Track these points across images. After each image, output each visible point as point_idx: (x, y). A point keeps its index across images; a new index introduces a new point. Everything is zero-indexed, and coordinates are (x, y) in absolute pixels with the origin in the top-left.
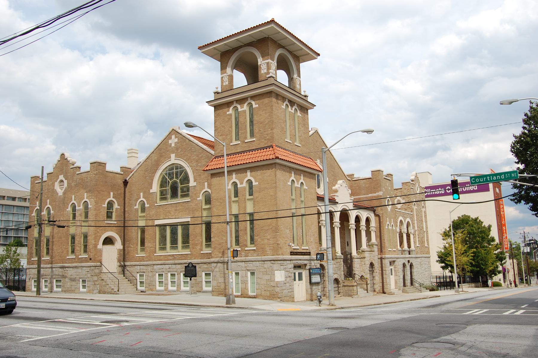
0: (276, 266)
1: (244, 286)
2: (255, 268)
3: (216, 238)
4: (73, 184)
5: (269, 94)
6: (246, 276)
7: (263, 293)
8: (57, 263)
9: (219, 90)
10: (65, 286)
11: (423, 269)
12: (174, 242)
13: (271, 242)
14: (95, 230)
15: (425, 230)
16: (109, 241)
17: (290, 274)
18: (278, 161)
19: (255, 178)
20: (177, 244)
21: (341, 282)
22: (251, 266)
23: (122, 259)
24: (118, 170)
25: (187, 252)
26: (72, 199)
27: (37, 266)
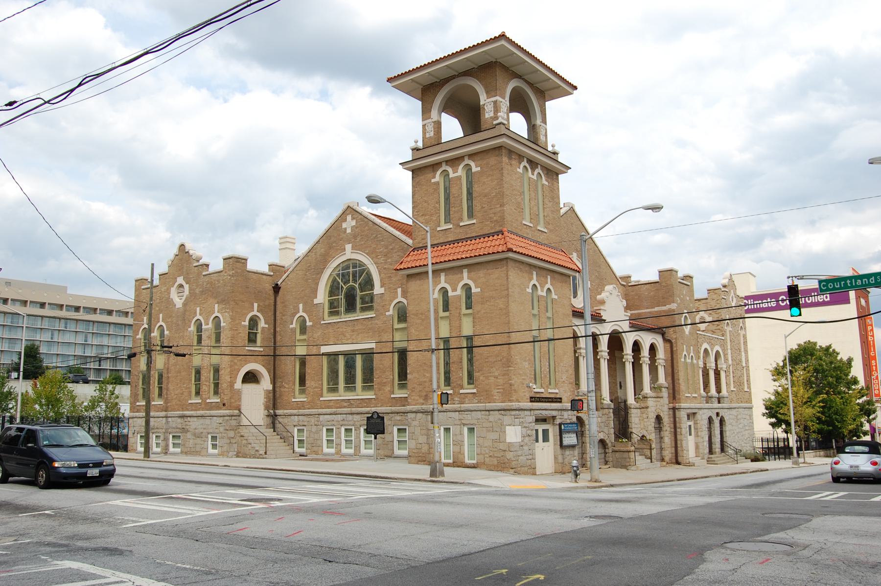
0: (507, 419)
1: (457, 449)
2: (475, 422)
3: (415, 375)
4: (197, 291)
5: (499, 148)
6: (461, 434)
7: (487, 460)
9: (420, 145)
11: (741, 426)
12: (350, 379)
13: (501, 381)
14: (232, 361)
15: (744, 365)
16: (251, 378)
17: (529, 432)
18: (511, 255)
19: (474, 281)
20: (354, 382)
21: (610, 445)
22: (468, 418)
23: (271, 406)
24: (265, 269)
25: (370, 395)
26: (195, 313)
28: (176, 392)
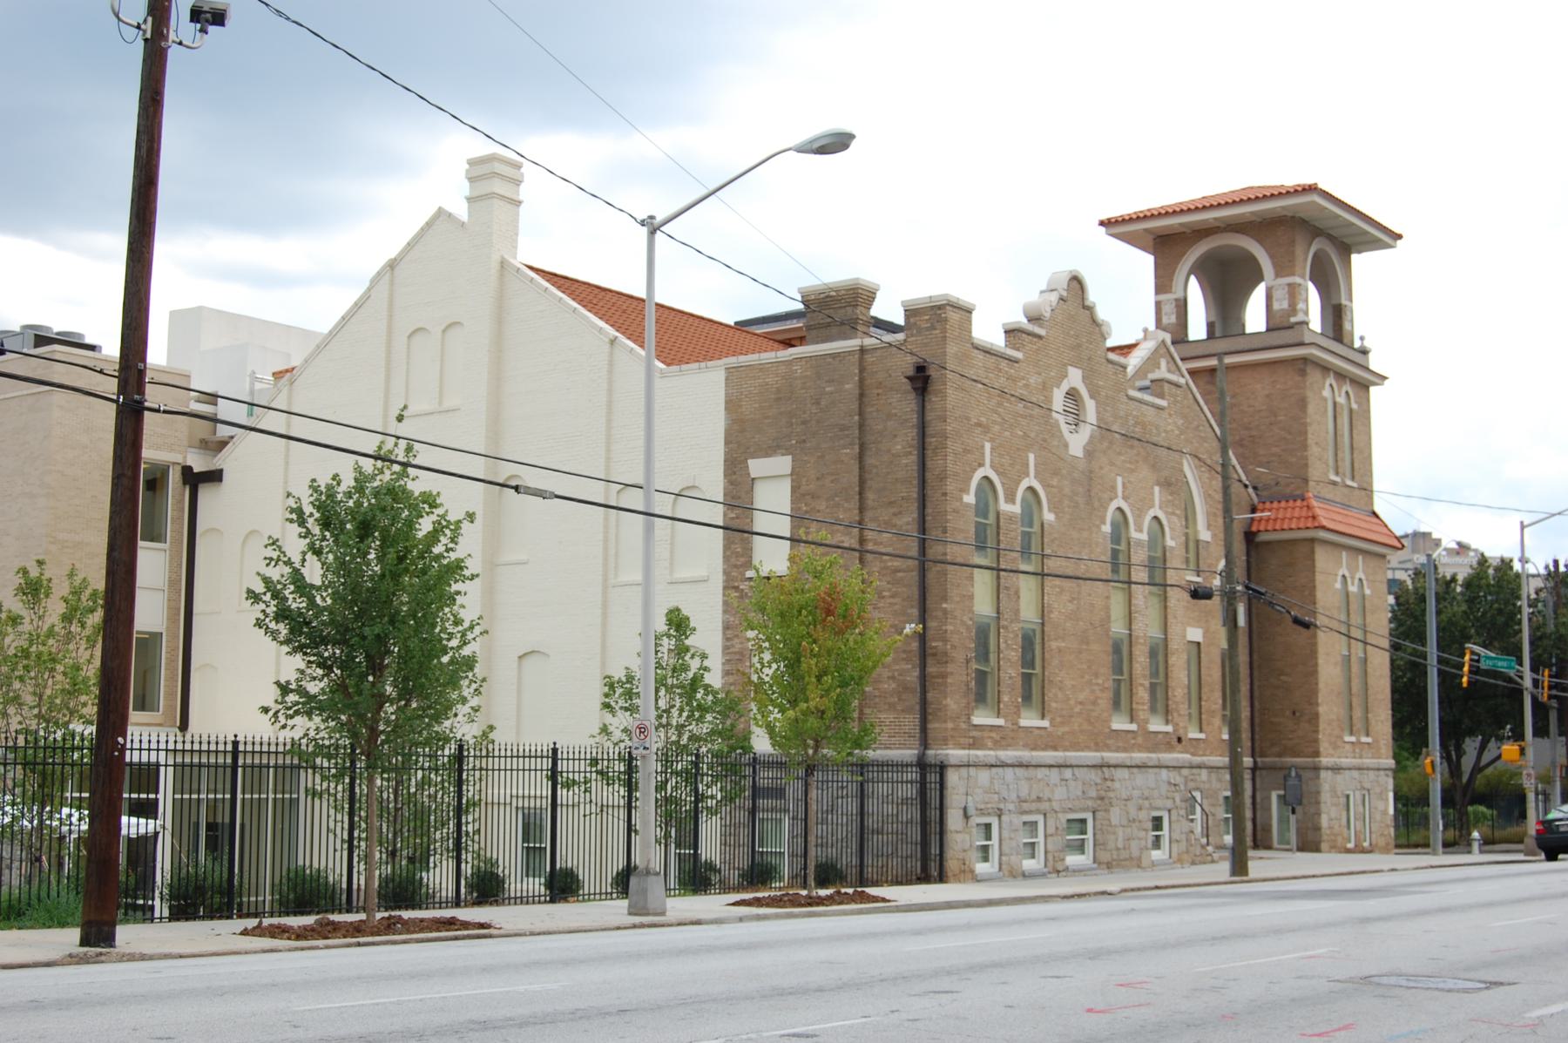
8: (1075, 746)
10: (1111, 845)
26: (1114, 488)
27: (1227, 759)
28: (1081, 697)
